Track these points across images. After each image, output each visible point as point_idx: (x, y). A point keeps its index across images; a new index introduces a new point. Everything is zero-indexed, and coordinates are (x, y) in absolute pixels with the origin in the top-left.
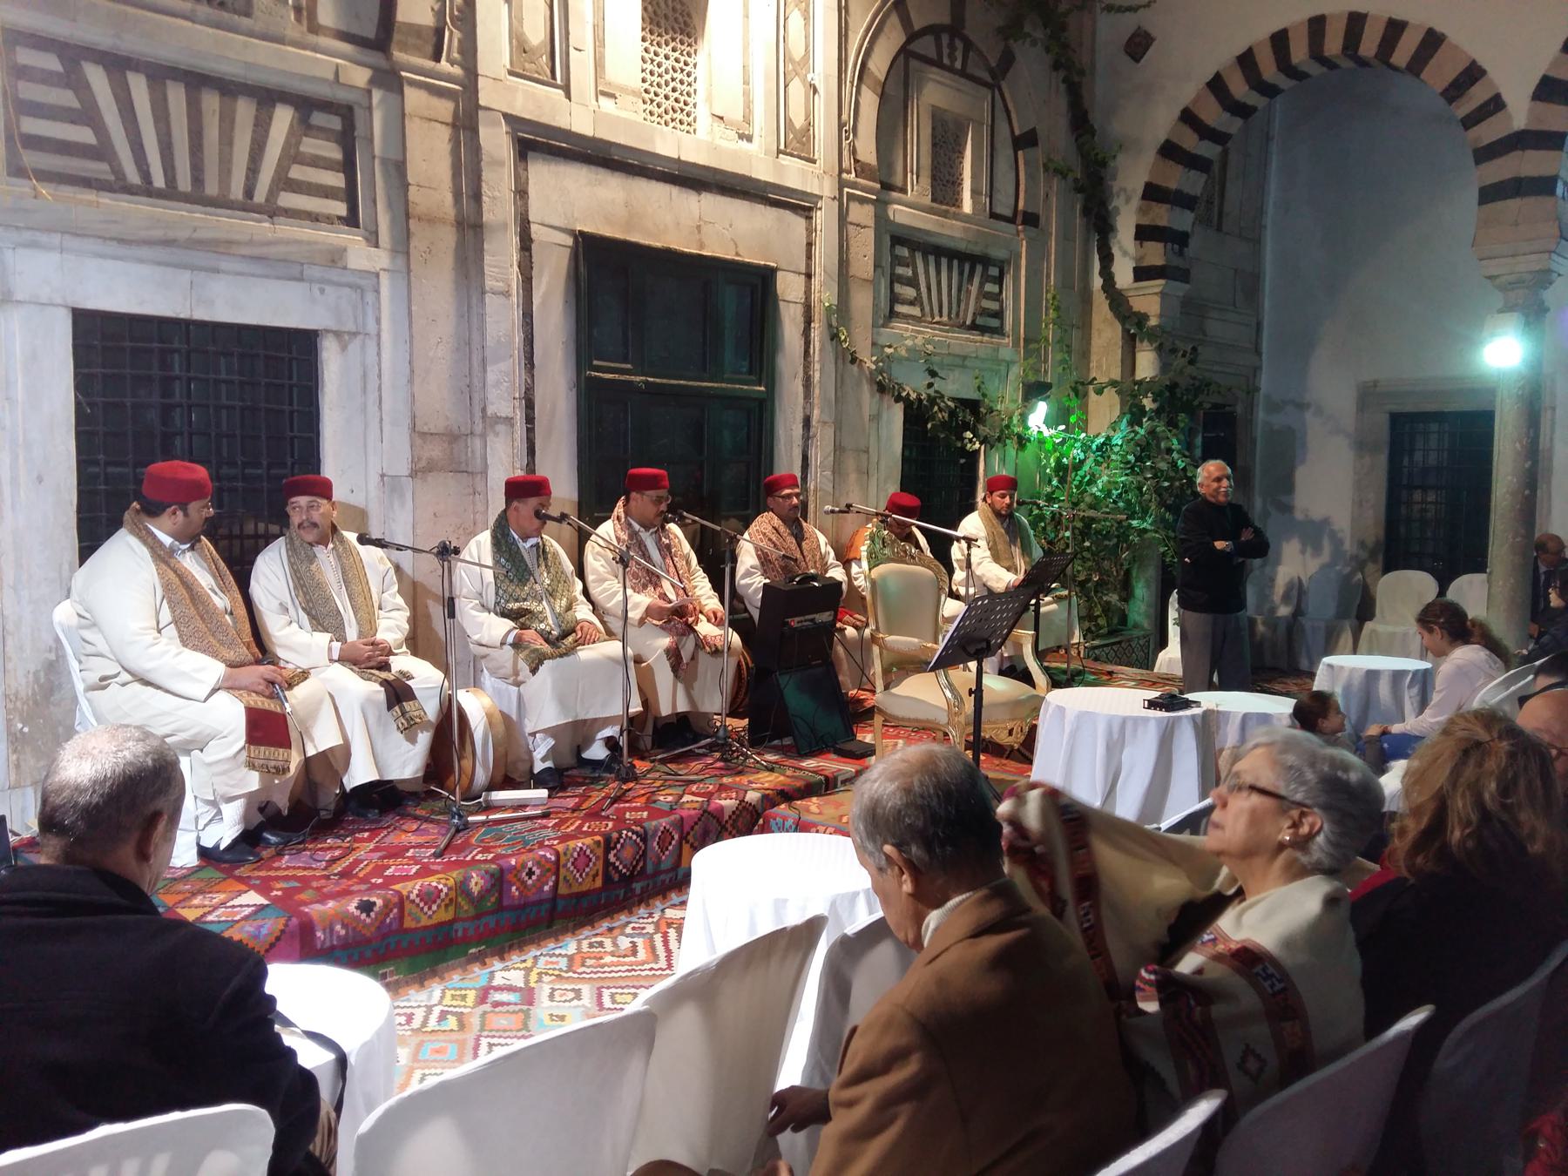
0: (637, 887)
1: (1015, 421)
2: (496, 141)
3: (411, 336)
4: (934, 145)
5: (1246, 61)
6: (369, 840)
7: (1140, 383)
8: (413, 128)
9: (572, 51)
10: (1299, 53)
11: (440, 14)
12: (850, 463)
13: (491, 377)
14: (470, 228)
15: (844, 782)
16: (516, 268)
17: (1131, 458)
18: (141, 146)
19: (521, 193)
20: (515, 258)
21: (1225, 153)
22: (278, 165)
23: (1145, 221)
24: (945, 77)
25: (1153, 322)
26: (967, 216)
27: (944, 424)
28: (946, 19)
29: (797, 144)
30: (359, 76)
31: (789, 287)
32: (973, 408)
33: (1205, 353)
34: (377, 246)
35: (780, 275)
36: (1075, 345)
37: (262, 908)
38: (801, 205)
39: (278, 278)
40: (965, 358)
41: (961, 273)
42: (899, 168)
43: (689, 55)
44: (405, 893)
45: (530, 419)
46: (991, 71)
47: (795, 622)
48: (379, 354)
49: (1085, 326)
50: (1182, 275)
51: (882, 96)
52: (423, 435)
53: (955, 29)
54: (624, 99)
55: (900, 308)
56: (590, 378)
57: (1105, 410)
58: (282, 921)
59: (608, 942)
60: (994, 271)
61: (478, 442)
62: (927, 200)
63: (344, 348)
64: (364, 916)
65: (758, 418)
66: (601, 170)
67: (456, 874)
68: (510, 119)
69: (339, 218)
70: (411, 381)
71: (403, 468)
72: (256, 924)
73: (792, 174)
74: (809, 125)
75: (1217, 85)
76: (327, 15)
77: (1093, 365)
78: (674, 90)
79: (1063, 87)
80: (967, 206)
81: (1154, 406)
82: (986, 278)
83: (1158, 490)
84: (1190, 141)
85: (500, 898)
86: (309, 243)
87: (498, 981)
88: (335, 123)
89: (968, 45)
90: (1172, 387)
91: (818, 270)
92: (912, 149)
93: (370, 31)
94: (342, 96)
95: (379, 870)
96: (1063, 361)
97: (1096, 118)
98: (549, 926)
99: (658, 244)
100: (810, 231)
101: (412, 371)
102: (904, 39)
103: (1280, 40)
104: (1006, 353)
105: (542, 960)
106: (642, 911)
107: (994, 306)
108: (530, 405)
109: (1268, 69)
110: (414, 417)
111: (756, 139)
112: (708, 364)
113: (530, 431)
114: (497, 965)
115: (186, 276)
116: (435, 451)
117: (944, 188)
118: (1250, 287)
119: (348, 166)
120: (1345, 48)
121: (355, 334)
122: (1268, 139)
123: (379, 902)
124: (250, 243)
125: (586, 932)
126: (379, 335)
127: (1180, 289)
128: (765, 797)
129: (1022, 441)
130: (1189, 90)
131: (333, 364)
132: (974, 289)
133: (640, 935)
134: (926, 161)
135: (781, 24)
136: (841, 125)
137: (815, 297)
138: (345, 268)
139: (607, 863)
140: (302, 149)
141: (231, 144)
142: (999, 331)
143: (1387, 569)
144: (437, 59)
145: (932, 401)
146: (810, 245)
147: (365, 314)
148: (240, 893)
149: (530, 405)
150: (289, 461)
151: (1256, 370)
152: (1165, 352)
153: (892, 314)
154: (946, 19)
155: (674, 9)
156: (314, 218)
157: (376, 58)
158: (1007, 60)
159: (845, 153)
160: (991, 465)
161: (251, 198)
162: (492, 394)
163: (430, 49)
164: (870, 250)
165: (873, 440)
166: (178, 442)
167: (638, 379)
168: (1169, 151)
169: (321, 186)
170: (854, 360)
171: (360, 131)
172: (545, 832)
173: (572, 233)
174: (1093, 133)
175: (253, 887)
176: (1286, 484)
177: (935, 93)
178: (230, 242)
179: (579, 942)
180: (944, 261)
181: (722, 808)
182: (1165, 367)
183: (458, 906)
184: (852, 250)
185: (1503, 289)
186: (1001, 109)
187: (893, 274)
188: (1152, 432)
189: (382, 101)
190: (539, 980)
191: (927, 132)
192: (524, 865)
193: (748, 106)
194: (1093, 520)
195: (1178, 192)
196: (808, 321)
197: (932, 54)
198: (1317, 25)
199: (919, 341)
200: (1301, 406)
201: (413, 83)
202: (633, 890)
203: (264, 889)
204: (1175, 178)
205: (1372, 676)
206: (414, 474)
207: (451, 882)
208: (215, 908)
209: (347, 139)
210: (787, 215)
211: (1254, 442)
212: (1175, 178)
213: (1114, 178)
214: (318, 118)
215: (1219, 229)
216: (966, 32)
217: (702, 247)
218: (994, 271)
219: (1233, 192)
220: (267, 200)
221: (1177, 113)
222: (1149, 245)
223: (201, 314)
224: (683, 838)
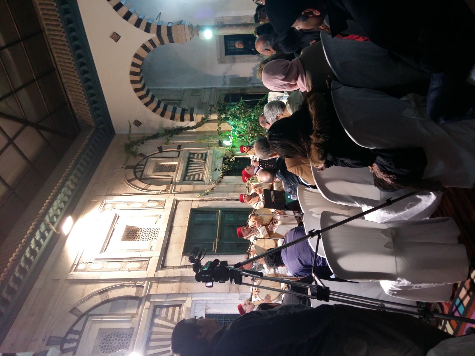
1: (228, 149)
2: (162, 274)
4: (162, 172)
5: (141, 98)
8: (159, 292)
10: (139, 86)
11: (133, 286)
12: (238, 189)
17: (237, 120)
18: (163, 352)
19: (173, 268)
21: (162, 100)
23: (179, 119)
24: (146, 169)
25: (204, 116)
27: (228, 167)
28: (132, 170)
29: (162, 204)
30: (147, 304)
31: (195, 205)
32: (225, 159)
33: (211, 103)
35: (192, 207)
36: (209, 135)
38: (176, 203)
41: (192, 164)
46: (144, 159)
47: (273, 200)
49: (205, 132)
50: (192, 110)
51: (151, 184)
53: (135, 168)
54: (152, 245)
55: (200, 178)
56: (217, 252)
60: (192, 156)
62: (175, 173)
63: (210, 308)
65: (226, 211)
68: (156, 271)
70: (217, 293)
71: (238, 295)
73: (169, 205)
74: (157, 201)
75: (147, 104)
76: (134, 311)
77: (214, 130)
79: (148, 141)
80: (176, 163)
81: (224, 115)
82: (193, 158)
83: (244, 113)
84: (160, 110)
88: (158, 309)
89: (138, 164)
90: (219, 111)
91: (191, 198)
92: (162, 177)
93: (137, 302)
94: (152, 308)
96: (213, 138)
97: (155, 133)
99: (185, 236)
100: (182, 200)
103: (136, 90)
109: (143, 92)
112: (214, 225)
117: (171, 169)
118: (195, 92)
119: (168, 307)
120: (138, 75)
121: (206, 306)
122: (159, 89)
127: (196, 110)
129: (233, 147)
130: (148, 111)
132: (196, 160)
134: (166, 173)
135: (135, 209)
136: (157, 194)
137: (197, 199)
141: (163, 332)
142: (206, 154)
144: (143, 287)
145: (223, 169)
146: (185, 201)
151: (216, 89)
153: (202, 180)
154: (132, 170)
157: (143, 300)
158: (142, 155)
159: (164, 193)
160: (240, 155)
163: (141, 288)
164: (187, 186)
165: (232, 184)
168: (162, 115)
170: (213, 189)
171: (160, 304)
173: (183, 256)
174: (158, 133)
176: (244, 79)
177: (149, 172)
180: (189, 168)
182: (215, 112)
184: (186, 190)
185: (193, 35)
188: (230, 115)
189: (153, 299)
194: (252, 128)
195: (172, 112)
196: (203, 200)
197: (140, 173)
198: (133, 82)
199: (208, 173)
200: (225, 77)
201: (149, 292)
204: (169, 113)
206: (239, 293)
209: (161, 307)
210: (178, 206)
211: (234, 88)
212: (169, 113)
214: (157, 313)
215: (181, 100)
216: (135, 165)
218: (192, 156)
219: (172, 97)
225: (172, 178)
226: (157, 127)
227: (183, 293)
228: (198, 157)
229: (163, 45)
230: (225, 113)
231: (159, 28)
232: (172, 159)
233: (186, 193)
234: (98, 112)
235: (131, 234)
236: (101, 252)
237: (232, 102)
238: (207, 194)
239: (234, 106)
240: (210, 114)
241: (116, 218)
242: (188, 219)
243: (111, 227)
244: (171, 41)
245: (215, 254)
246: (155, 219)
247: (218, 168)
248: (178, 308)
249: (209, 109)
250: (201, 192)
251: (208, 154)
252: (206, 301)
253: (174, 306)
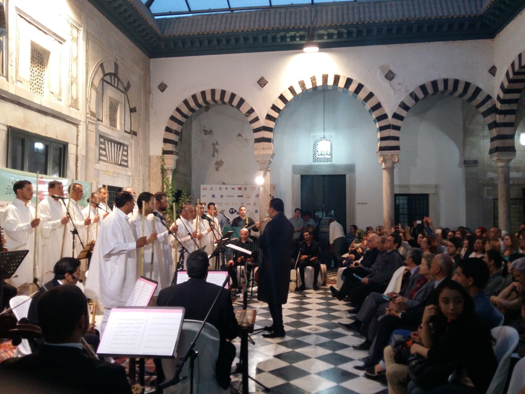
9: (9, 66)
28: (113, 71)
29: (74, 104)
31: (72, 149)
35: (69, 145)
41: (117, 148)
43: (42, 71)
55: (102, 158)
60: (125, 148)
66: (17, 106)
73: (73, 113)
78: (38, 82)
82: (124, 150)
84: (179, 117)
89: (119, 80)
92: (105, 109)
100: (78, 131)
102: (102, 76)
130: (178, 102)
132: (121, 153)
134: (108, 113)
136: (87, 99)
137: (79, 153)
142: (127, 166)
146: (78, 136)
155: (39, 56)
164: (94, 139)
177: (110, 92)
180: (113, 144)
193: (60, 90)
196: (77, 160)
197: (109, 81)
217: (47, 133)
222: (167, 144)
225: (102, 121)
228: (123, 155)
232: (123, 123)
234: (180, 44)
235: (39, 57)
236: (17, 9)
241: (61, 40)
242: (55, 137)
243: (49, 31)
244: (258, 140)
251: (127, 168)
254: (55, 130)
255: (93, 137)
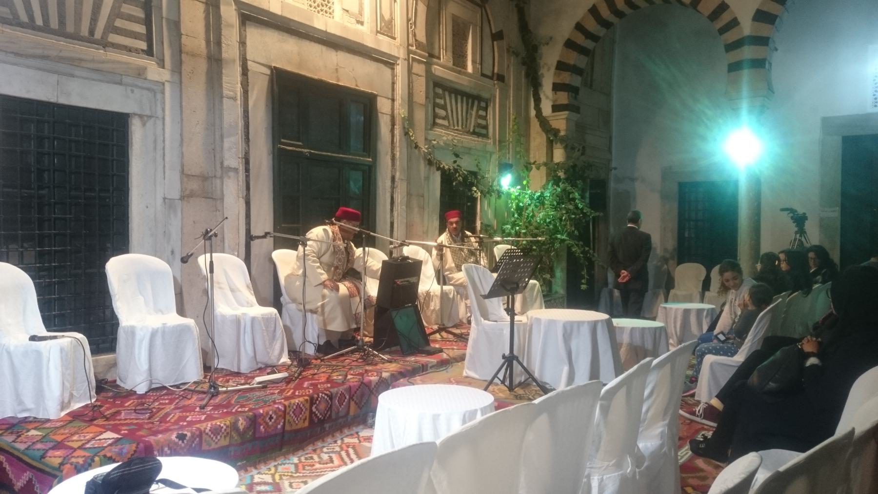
0: (327, 426)
3: (182, 120)
4: (453, 35)
6: (170, 403)
7: (558, 164)
12: (415, 202)
13: (227, 144)
14: (215, 61)
15: (431, 367)
16: (239, 85)
19: (243, 43)
20: (239, 79)
22: (108, 18)
23: (558, 81)
25: (562, 133)
26: (470, 74)
29: (386, 28)
31: (383, 106)
34: (163, 67)
35: (379, 99)
37: (118, 440)
38: (388, 62)
39: (108, 82)
40: (470, 149)
41: (467, 105)
42: (437, 46)
44: (203, 429)
45: (247, 170)
47: (399, 282)
48: (164, 129)
52: (188, 176)
57: (539, 176)
58: (135, 445)
59: (315, 457)
60: (483, 104)
61: (218, 181)
62: (450, 64)
63: (144, 125)
64: (180, 442)
66: (285, 34)
67: (228, 420)
69: (143, 50)
71: (175, 194)
72: (119, 447)
73: (385, 45)
74: (392, 20)
80: (470, 69)
82: (480, 108)
84: (580, 39)
85: (254, 433)
86: (125, 63)
87: (257, 479)
90: (574, 167)
95: (183, 419)
98: (280, 450)
99: (316, 77)
100: (394, 76)
101: (182, 140)
104: (490, 148)
105: (280, 468)
106: (329, 440)
107: (483, 122)
108: (247, 162)
110: (182, 166)
111: (365, 24)
113: (247, 177)
114: (254, 472)
115: (55, 77)
116: (194, 185)
119: (148, 22)
121: (150, 117)
123: (189, 434)
124: (93, 61)
125: (300, 453)
126: (164, 118)
127: (575, 116)
128: (392, 375)
129: (499, 194)
131: (137, 134)
132: (474, 113)
133: (332, 452)
134: (450, 44)
136: (408, 20)
138: (146, 79)
139: (311, 412)
140: (122, 10)
142: (486, 136)
143: (680, 263)
145: (456, 171)
147: (156, 106)
148: (101, 433)
149: (247, 162)
150: (111, 189)
152: (569, 149)
153: (434, 124)
156: (129, 50)
159: (410, 35)
161: (93, 36)
162: (227, 155)
164: (423, 89)
166: (46, 175)
167: (306, 150)
169: (133, 32)
170: (417, 147)
172: (274, 397)
173: (269, 67)
175: (107, 430)
178: (81, 60)
179: (299, 457)
181: (370, 382)
182: (568, 157)
183: (231, 437)
184: (415, 88)
186: (485, 19)
187: (434, 103)
188: (564, 190)
190: (281, 479)
191: (450, 28)
192: (267, 413)
195: (574, 66)
196: (393, 124)
199: (450, 137)
200: (633, 180)
202: (324, 429)
203: (115, 429)
204: (573, 58)
205: (687, 312)
206: (182, 198)
207: (228, 423)
208: (89, 441)
210: (381, 66)
212: (573, 58)
213: (541, 58)
215: (591, 87)
217: (338, 80)
220: (102, 38)
221: (573, 25)
223: (63, 100)
224: (351, 398)
226: (543, 32)
227: (181, 62)
228: (480, 117)
229: (723, 49)
230: (567, 179)
231: (762, 41)
232: (478, 61)
233: (409, 86)
237: (590, 194)
238: (406, 134)
239: (583, 197)
240: (566, 148)
242: (353, 86)
245: (274, 147)
246: (355, 10)
247: (458, 160)
248: (145, 48)
249: (576, 145)
250: (410, 120)
252: (161, 116)
253: (149, 39)
254: (352, 73)
255: (420, 85)
